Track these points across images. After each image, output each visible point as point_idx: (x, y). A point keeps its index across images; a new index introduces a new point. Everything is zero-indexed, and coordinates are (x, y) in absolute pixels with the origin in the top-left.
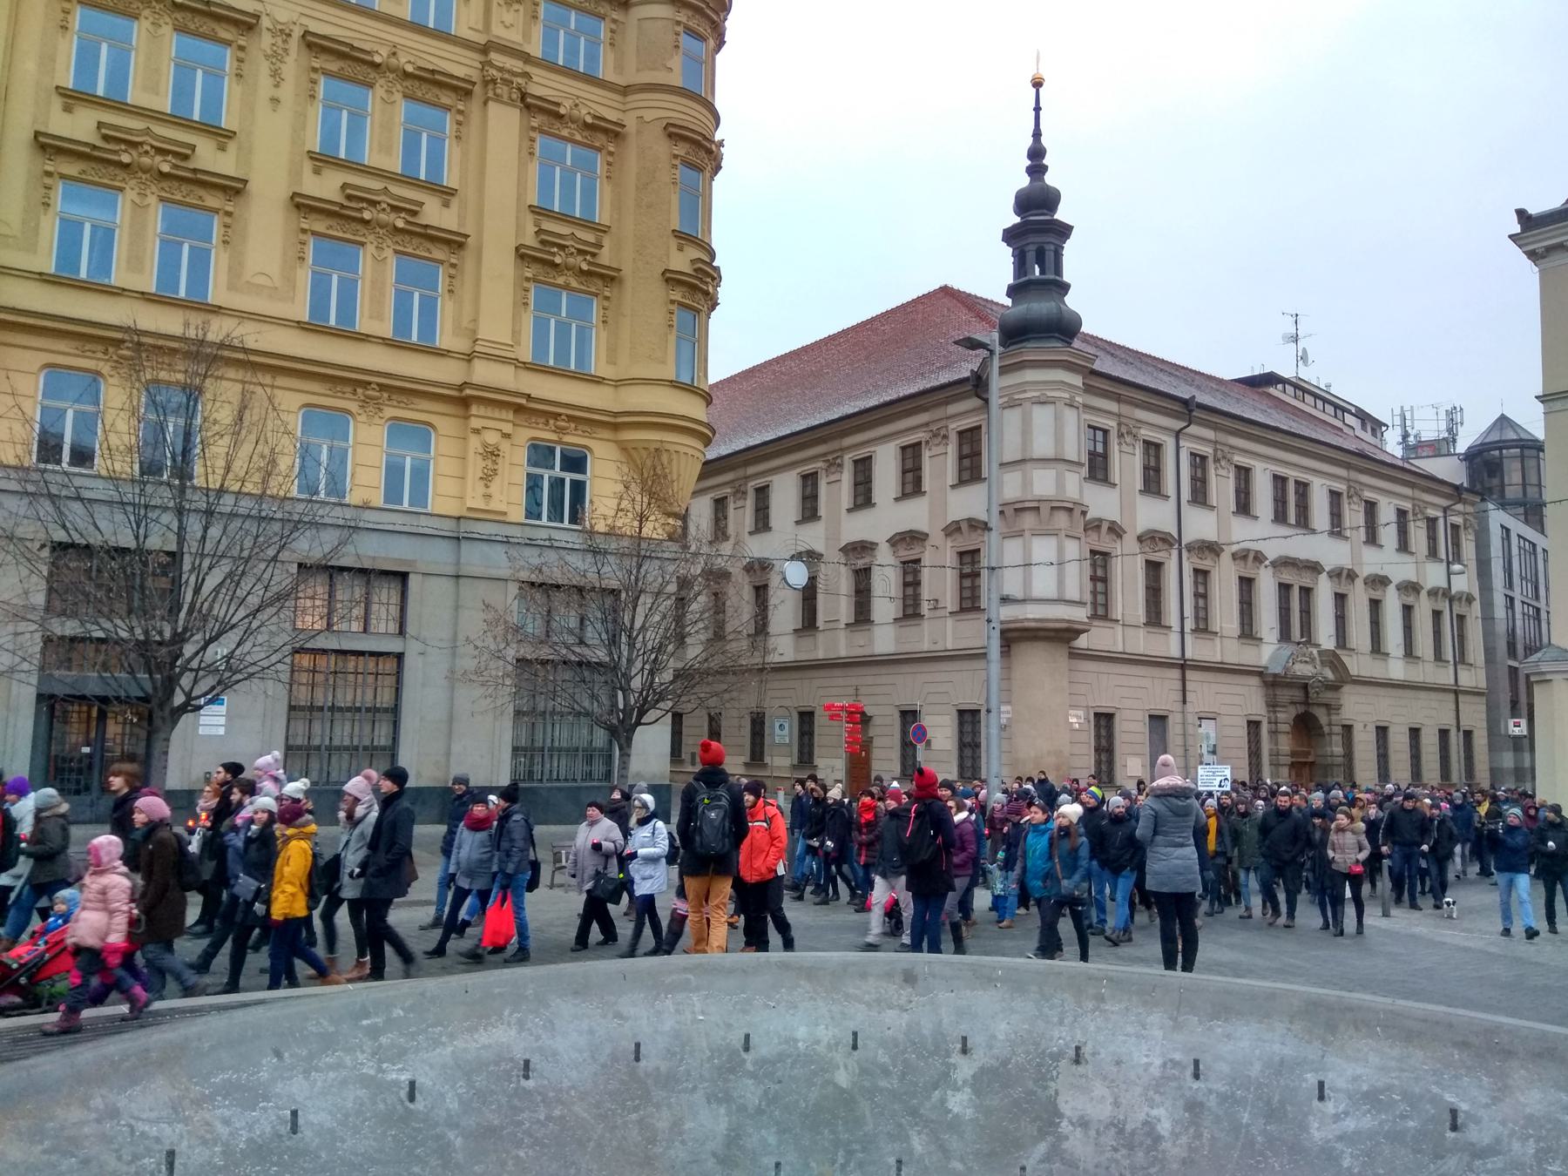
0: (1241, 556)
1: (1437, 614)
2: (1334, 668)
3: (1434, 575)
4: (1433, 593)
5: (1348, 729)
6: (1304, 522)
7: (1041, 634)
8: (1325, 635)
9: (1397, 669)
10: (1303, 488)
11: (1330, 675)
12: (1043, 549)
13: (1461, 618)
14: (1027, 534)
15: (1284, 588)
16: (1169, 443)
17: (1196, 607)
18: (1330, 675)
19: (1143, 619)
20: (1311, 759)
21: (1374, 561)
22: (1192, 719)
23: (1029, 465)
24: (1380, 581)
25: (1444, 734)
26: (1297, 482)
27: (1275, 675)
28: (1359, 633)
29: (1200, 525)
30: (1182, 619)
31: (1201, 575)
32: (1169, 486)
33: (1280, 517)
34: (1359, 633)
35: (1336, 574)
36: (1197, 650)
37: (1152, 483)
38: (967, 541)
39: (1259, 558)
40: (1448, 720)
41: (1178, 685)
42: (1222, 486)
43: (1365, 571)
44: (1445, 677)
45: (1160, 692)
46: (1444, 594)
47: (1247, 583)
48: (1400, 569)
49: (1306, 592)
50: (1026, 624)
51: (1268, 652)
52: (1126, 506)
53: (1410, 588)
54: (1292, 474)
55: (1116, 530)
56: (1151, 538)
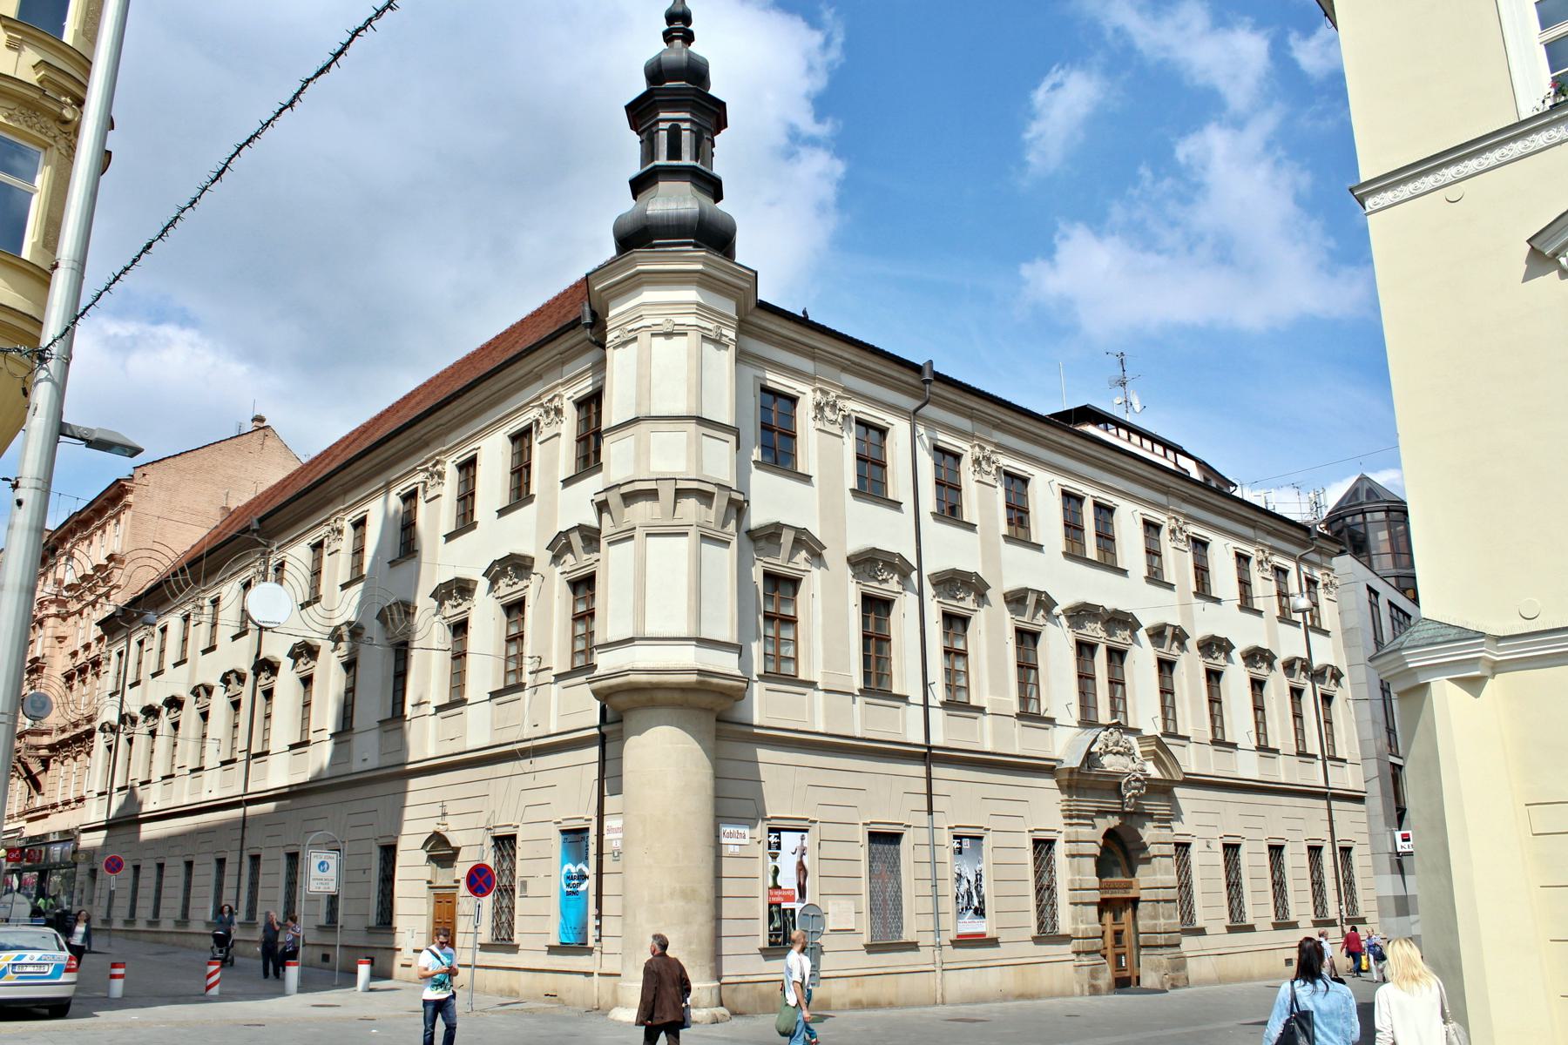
0: (1016, 600)
1: (1296, 693)
2: (1158, 762)
3: (1289, 643)
4: (1289, 666)
5: (1182, 848)
6: (1108, 562)
7: (660, 696)
8: (1145, 713)
9: (1248, 766)
10: (1104, 511)
11: (1153, 771)
12: (670, 559)
13: (1327, 699)
14: (637, 533)
15: (1085, 649)
16: (899, 430)
17: (950, 673)
18: (1153, 771)
19: (857, 682)
20: (1132, 894)
21: (1204, 622)
22: (945, 838)
23: (643, 427)
24: (1214, 646)
25: (1315, 851)
26: (1097, 505)
27: (1071, 771)
28: (1192, 716)
29: (947, 549)
30: (926, 685)
31: (955, 622)
32: (898, 485)
33: (1074, 553)
34: (1192, 716)
35: (1157, 634)
36: (945, 732)
37: (871, 481)
38: (576, 562)
39: (1045, 603)
40: (1320, 832)
41: (922, 786)
42: (983, 499)
43: (1197, 633)
44: (1313, 775)
45: (890, 794)
46: (1303, 668)
47: (1027, 638)
48: (1245, 632)
49: (1117, 656)
50: (633, 678)
51: (1064, 744)
52: (831, 513)
53: (1256, 656)
54: (1089, 492)
55: (805, 542)
56: (867, 562)
